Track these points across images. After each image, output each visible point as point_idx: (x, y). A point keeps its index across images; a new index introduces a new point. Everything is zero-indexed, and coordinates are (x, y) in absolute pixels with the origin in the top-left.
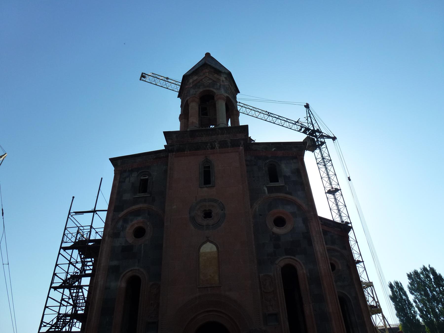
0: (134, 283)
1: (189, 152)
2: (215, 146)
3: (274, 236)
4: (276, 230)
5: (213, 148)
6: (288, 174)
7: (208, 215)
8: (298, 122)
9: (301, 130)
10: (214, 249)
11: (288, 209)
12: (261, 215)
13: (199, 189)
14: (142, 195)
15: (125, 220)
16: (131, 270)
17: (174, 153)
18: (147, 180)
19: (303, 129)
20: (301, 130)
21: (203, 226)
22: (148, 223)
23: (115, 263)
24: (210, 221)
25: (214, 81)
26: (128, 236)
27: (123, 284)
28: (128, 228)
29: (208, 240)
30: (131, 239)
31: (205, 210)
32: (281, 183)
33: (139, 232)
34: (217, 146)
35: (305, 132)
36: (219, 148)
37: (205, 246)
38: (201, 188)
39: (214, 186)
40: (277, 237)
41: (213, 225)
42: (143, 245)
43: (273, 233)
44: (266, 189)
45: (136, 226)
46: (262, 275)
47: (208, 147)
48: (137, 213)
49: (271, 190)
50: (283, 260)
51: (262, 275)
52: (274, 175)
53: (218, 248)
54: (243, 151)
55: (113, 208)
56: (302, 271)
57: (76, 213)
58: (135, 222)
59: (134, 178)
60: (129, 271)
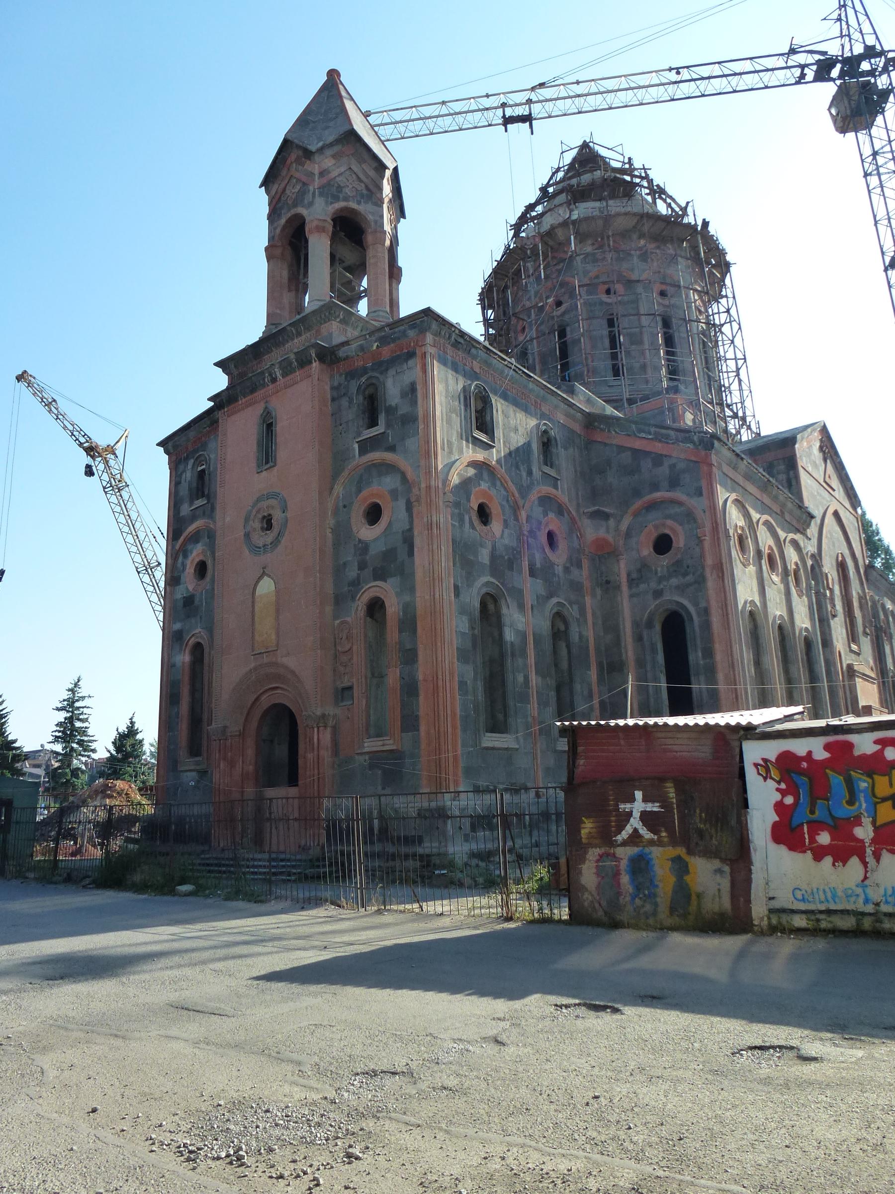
4: (367, 533)
5: (274, 380)
7: (268, 522)
8: (793, 51)
11: (390, 482)
12: (345, 506)
18: (203, 471)
19: (810, 74)
20: (803, 76)
23: (177, 626)
24: (270, 537)
25: (304, 184)
34: (278, 374)
35: (822, 74)
37: (261, 583)
40: (363, 548)
43: (360, 540)
44: (356, 446)
45: (197, 560)
46: (338, 622)
51: (338, 622)
52: (372, 408)
56: (393, 607)
58: (195, 553)
59: (188, 475)
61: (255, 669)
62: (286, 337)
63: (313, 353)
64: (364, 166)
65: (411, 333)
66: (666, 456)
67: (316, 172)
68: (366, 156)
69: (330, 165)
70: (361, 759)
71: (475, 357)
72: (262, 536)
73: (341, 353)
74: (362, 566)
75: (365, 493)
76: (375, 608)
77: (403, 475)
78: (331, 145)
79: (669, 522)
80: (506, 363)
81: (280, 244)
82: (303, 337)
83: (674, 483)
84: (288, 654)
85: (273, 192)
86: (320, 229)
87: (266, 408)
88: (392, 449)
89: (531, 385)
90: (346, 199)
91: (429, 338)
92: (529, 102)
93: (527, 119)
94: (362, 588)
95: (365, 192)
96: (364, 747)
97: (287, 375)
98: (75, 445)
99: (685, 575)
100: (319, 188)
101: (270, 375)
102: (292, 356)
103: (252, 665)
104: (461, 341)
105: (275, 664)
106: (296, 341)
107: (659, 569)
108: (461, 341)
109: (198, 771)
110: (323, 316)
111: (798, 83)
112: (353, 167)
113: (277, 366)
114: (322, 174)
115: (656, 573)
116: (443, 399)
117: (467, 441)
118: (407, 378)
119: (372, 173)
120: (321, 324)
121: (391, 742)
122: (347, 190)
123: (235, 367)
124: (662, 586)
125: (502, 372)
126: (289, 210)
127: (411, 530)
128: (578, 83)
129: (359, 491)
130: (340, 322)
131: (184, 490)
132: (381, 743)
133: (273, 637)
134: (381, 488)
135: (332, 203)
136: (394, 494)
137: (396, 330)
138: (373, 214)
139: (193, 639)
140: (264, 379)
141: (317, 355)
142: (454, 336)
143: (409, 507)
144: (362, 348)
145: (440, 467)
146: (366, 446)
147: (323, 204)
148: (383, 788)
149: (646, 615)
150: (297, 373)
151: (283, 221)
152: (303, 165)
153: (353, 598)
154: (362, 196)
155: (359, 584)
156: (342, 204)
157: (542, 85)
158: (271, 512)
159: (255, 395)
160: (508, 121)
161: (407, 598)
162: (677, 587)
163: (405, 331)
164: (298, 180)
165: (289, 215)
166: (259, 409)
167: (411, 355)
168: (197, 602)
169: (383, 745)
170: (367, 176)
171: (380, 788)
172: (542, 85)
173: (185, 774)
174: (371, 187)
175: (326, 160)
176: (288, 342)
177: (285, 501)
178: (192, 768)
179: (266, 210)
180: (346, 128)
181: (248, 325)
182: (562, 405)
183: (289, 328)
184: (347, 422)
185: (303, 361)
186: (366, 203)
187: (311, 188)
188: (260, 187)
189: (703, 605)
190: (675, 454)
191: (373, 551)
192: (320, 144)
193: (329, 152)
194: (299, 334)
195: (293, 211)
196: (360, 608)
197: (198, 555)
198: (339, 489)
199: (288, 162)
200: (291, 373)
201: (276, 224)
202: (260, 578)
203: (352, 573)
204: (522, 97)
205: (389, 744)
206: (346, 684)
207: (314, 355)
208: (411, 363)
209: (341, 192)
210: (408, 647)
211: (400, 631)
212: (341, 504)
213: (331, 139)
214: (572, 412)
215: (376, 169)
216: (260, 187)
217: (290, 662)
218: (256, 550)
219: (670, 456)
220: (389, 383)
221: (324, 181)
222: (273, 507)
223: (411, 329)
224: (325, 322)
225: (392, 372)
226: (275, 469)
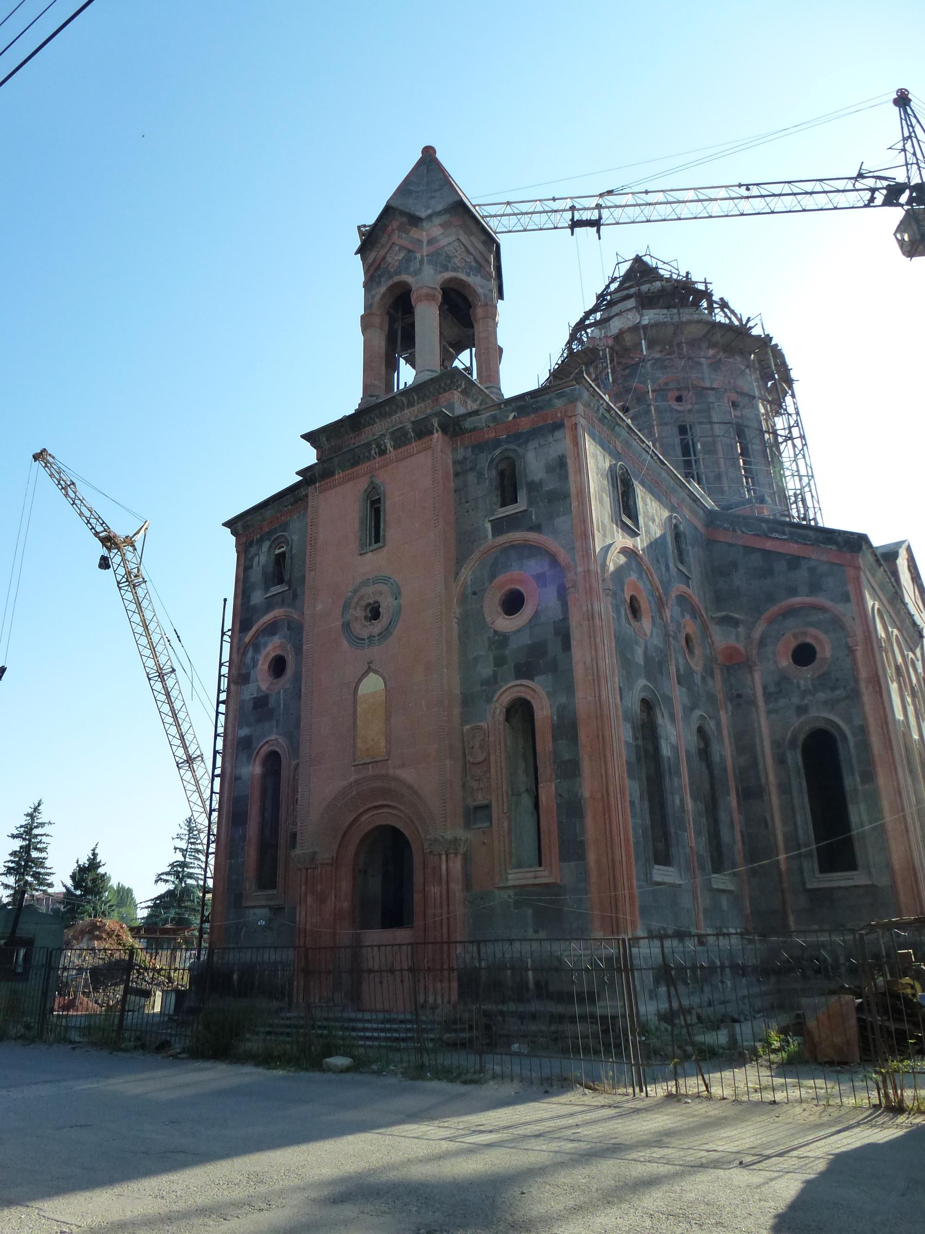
2: (386, 446)
3: (497, 637)
4: (505, 624)
5: (383, 452)
7: (374, 613)
8: (861, 176)
9: (872, 199)
11: (534, 566)
12: (474, 593)
14: (278, 589)
15: (257, 648)
16: (267, 742)
18: (283, 555)
19: (880, 197)
20: (872, 199)
21: (364, 640)
23: (244, 732)
24: (377, 627)
25: (409, 251)
26: (261, 680)
27: (257, 769)
34: (388, 445)
35: (892, 198)
36: (395, 448)
37: (365, 681)
38: (361, 554)
40: (501, 640)
43: (495, 632)
44: (488, 526)
45: (273, 655)
46: (468, 727)
47: (373, 452)
49: (500, 527)
51: (468, 727)
52: (508, 485)
55: (237, 627)
56: (544, 712)
58: (270, 647)
59: (263, 558)
60: (263, 745)
61: (357, 782)
62: (394, 408)
63: (435, 422)
64: (472, 238)
65: (558, 403)
66: (804, 558)
67: (425, 239)
68: (474, 229)
69: (438, 233)
70: (504, 894)
71: (618, 435)
72: (365, 626)
73: (468, 424)
74: (500, 662)
75: (501, 578)
76: (520, 712)
77: (553, 560)
78: (439, 214)
79: (812, 631)
80: (644, 446)
81: (378, 313)
82: (416, 408)
83: (815, 587)
84: (403, 765)
85: (370, 260)
86: (430, 297)
87: (372, 482)
88: (537, 528)
89: (664, 474)
90: (455, 269)
91: (580, 408)
92: (599, 207)
93: (596, 224)
94: (501, 686)
95: (474, 264)
96: (507, 880)
97: (400, 447)
98: (90, 534)
99: (833, 689)
100: (428, 256)
101: (378, 446)
102: (409, 426)
103: (353, 778)
104: (607, 415)
106: (406, 411)
107: (802, 682)
108: (607, 415)
109: (270, 908)
110: (443, 385)
111: (866, 206)
112: (462, 238)
113: (388, 436)
114: (430, 242)
115: (798, 686)
116: (595, 475)
117: (617, 525)
118: (554, 451)
119: (480, 246)
120: (440, 393)
121: (546, 873)
122: (456, 260)
123: (327, 439)
124: (806, 701)
125: (640, 455)
126: (390, 277)
127: (565, 619)
128: (647, 192)
129: (493, 576)
130: (461, 392)
131: (256, 574)
132: (532, 875)
134: (522, 574)
135: (440, 272)
136: (541, 579)
137: (539, 399)
138: (482, 287)
139: (266, 746)
141: (440, 425)
142: (601, 410)
143: (562, 593)
144: (494, 418)
145: (598, 550)
146: (500, 527)
147: (432, 272)
148: (536, 932)
149: (789, 735)
150: (414, 444)
151: (383, 289)
152: (408, 232)
153: (489, 700)
154: (471, 268)
155: (496, 682)
156: (448, 275)
157: (610, 192)
159: (357, 468)
160: (575, 224)
161: (563, 699)
162: (825, 703)
163: (550, 400)
164: (402, 248)
165: (391, 283)
166: (363, 484)
167: (558, 426)
168: (272, 702)
169: (536, 877)
170: (476, 248)
171: (530, 931)
172: (610, 192)
173: (252, 911)
174: (480, 260)
175: (434, 229)
176: (396, 413)
177: (398, 586)
178: (263, 903)
179: (362, 279)
180: (454, 199)
181: (344, 397)
182: (688, 500)
183: (398, 398)
184: (475, 500)
185: (422, 430)
186: (475, 275)
187: (418, 255)
188: (356, 254)
189: (857, 722)
190: (814, 556)
192: (430, 211)
193: (437, 221)
194: (411, 404)
195: (396, 279)
196: (498, 711)
197: (273, 650)
198: (466, 574)
199: (390, 228)
200: (405, 444)
201: (373, 292)
202: (365, 675)
203: (486, 670)
204: (593, 202)
205: (545, 876)
206: (480, 799)
207: (436, 425)
208: (558, 434)
209: (450, 261)
210: (566, 757)
211: (555, 739)
212: (469, 591)
213: (439, 208)
214: (697, 508)
215: (484, 243)
216: (356, 254)
217: (407, 775)
218: (357, 641)
219: (809, 559)
220: (531, 456)
221: (432, 249)
222: (381, 593)
223: (558, 398)
224: (445, 391)
225: (532, 445)
226: (385, 549)
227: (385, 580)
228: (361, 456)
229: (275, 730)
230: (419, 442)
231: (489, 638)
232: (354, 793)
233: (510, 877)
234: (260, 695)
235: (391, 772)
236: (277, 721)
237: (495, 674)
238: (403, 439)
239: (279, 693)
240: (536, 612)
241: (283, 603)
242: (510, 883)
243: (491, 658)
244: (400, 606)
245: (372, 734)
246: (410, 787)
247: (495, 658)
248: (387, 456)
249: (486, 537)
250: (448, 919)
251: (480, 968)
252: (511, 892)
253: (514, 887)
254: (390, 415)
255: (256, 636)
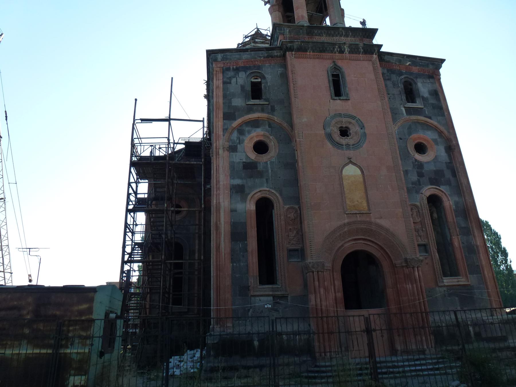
0: (264, 207)
1: (311, 53)
3: (417, 163)
4: (419, 157)
5: (342, 52)
6: (426, 95)
7: (344, 132)
10: (358, 172)
13: (331, 100)
14: (257, 102)
16: (260, 191)
17: (293, 53)
18: (260, 83)
21: (343, 145)
22: (271, 137)
23: (237, 182)
27: (251, 207)
28: (246, 141)
29: (351, 161)
30: (253, 156)
31: (341, 127)
32: (418, 104)
33: (261, 147)
34: (346, 49)
36: (349, 53)
37: (347, 168)
39: (349, 100)
40: (420, 165)
41: (353, 145)
42: (269, 162)
43: (416, 160)
45: (256, 140)
47: (336, 49)
48: (255, 124)
49: (409, 111)
50: (428, 190)
52: (410, 94)
53: (362, 172)
54: (378, 60)
57: (143, 120)
58: (253, 134)
59: (243, 79)
61: (349, 224)
62: (337, 33)
70: (442, 289)
74: (420, 175)
75: (414, 136)
76: (434, 201)
82: (349, 39)
96: (443, 282)
97: (353, 53)
103: (346, 221)
105: (370, 223)
106: (342, 38)
109: (274, 297)
113: (348, 45)
123: (289, 32)
129: (410, 134)
132: (456, 280)
133: (365, 204)
139: (259, 194)
140: (334, 48)
146: (409, 111)
155: (420, 185)
158: (350, 126)
163: (428, 64)
168: (260, 168)
169: (458, 282)
173: (258, 298)
176: (337, 36)
178: (271, 293)
183: (341, 29)
184: (393, 94)
191: (426, 168)
194: (347, 36)
200: (356, 53)
203: (414, 178)
205: (462, 281)
211: (456, 217)
217: (383, 222)
218: (338, 145)
222: (350, 123)
226: (350, 102)
227: (353, 117)
228: (328, 49)
229: (265, 185)
230: (364, 56)
231: (413, 162)
232: (346, 229)
233: (445, 281)
234: (249, 161)
235: (373, 220)
236: (267, 180)
237: (419, 181)
238: (356, 50)
239: (266, 162)
240: (436, 156)
241: (263, 111)
242: (446, 284)
243: (416, 173)
244: (365, 133)
245: (356, 198)
246: (387, 230)
247: (418, 173)
248: (344, 55)
249: (403, 114)
250: (423, 301)
251: (442, 326)
252: (445, 289)
253: (447, 286)
254: (333, 36)
255: (240, 125)
